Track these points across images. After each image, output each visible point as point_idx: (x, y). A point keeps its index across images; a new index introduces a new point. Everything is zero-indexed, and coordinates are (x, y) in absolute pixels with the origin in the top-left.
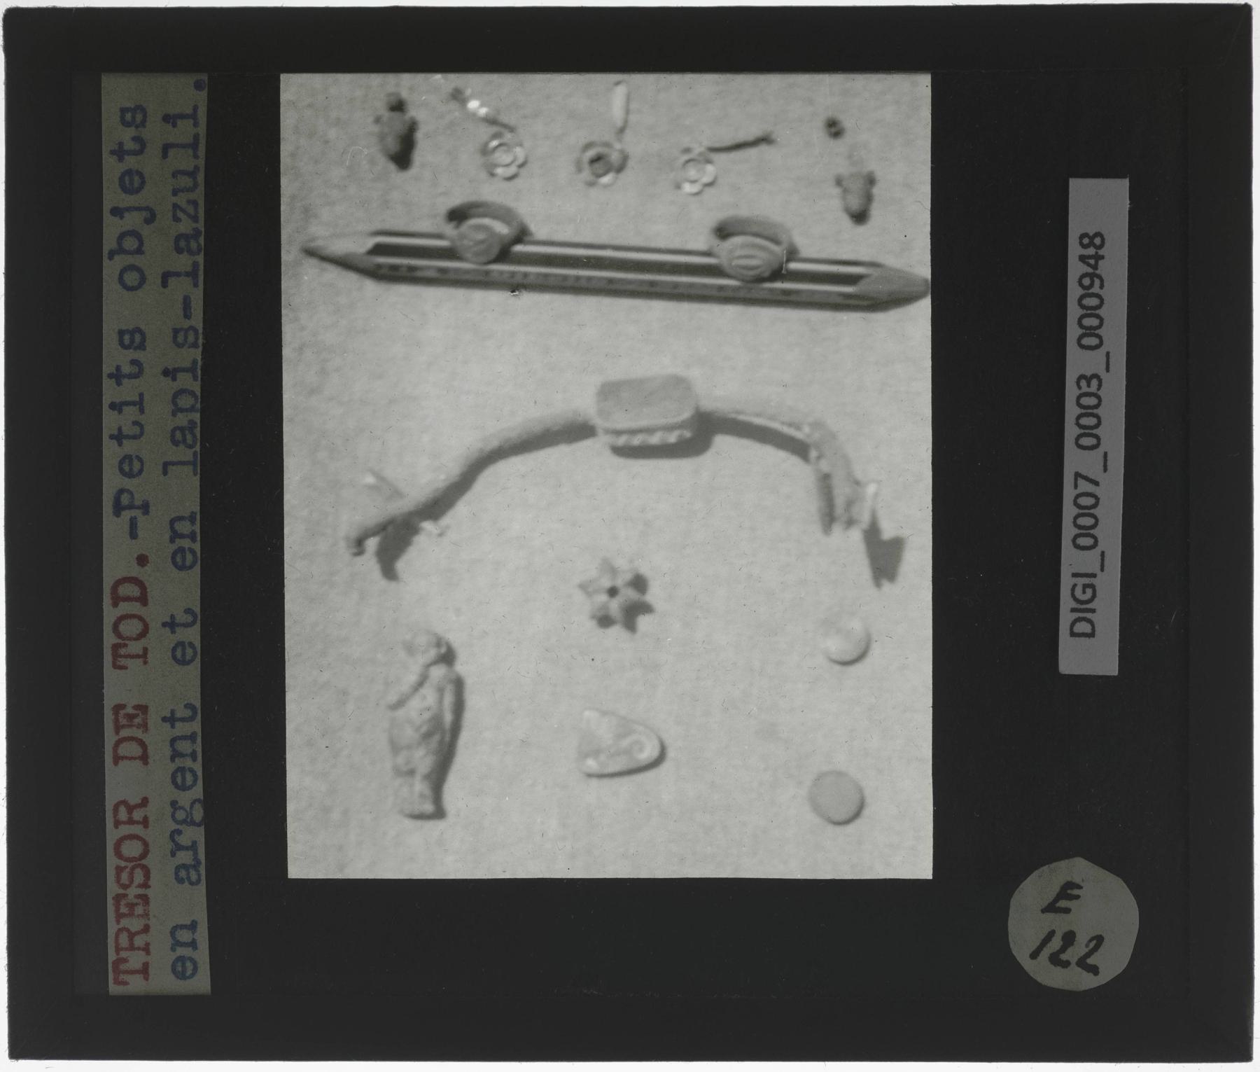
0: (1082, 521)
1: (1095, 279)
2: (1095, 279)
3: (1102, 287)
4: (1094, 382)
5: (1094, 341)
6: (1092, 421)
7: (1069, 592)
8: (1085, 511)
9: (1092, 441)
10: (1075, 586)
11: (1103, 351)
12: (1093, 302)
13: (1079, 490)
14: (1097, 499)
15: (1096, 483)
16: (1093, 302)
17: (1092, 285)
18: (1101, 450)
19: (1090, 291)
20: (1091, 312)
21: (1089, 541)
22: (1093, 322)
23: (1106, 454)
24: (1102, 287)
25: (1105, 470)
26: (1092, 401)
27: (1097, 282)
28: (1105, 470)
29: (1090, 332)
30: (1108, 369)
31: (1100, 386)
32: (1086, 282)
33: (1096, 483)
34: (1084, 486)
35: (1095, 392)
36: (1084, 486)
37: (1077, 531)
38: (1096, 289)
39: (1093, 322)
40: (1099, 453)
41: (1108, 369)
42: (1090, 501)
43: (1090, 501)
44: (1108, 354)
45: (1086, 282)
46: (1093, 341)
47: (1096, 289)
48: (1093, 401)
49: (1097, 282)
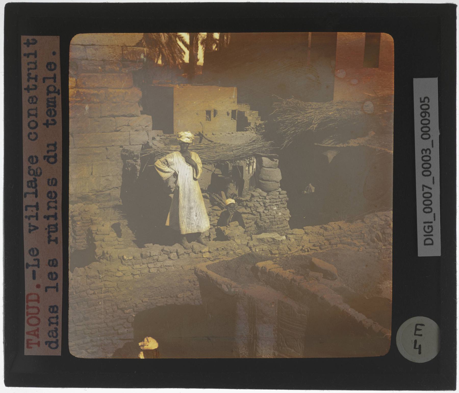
0: (426, 203)
1: (427, 113)
2: (427, 113)
3: (429, 116)
4: (428, 151)
5: (427, 136)
6: (428, 166)
7: (423, 228)
8: (427, 199)
9: (428, 173)
10: (425, 227)
11: (430, 140)
12: (426, 122)
13: (425, 191)
14: (430, 193)
15: (431, 189)
16: (427, 122)
17: (425, 116)
18: (432, 176)
19: (425, 118)
20: (426, 126)
21: (429, 210)
22: (426, 129)
23: (433, 178)
24: (429, 116)
25: (434, 183)
26: (428, 158)
27: (427, 115)
28: (434, 183)
29: (426, 133)
30: (433, 146)
31: (430, 153)
32: (423, 115)
33: (431, 189)
34: (426, 190)
35: (429, 155)
36: (426, 190)
37: (425, 206)
38: (427, 117)
39: (426, 129)
40: (431, 178)
41: (433, 146)
42: (429, 195)
43: (429, 195)
44: (432, 141)
45: (423, 115)
46: (427, 136)
47: (427, 117)
48: (428, 158)
49: (427, 115)
